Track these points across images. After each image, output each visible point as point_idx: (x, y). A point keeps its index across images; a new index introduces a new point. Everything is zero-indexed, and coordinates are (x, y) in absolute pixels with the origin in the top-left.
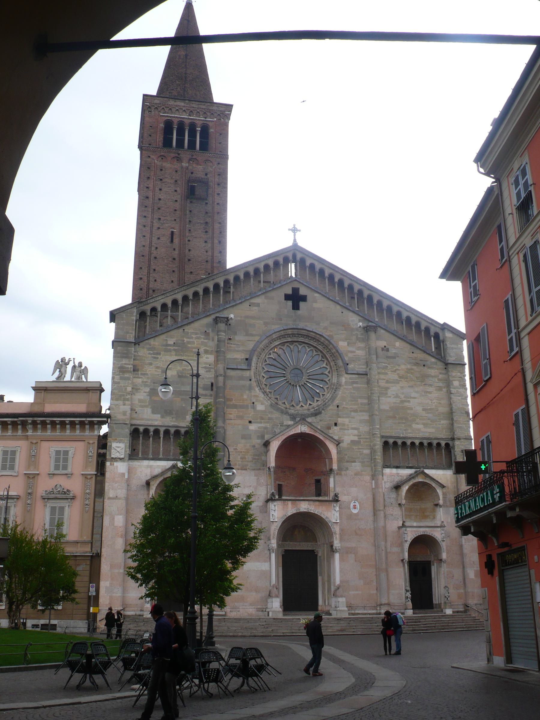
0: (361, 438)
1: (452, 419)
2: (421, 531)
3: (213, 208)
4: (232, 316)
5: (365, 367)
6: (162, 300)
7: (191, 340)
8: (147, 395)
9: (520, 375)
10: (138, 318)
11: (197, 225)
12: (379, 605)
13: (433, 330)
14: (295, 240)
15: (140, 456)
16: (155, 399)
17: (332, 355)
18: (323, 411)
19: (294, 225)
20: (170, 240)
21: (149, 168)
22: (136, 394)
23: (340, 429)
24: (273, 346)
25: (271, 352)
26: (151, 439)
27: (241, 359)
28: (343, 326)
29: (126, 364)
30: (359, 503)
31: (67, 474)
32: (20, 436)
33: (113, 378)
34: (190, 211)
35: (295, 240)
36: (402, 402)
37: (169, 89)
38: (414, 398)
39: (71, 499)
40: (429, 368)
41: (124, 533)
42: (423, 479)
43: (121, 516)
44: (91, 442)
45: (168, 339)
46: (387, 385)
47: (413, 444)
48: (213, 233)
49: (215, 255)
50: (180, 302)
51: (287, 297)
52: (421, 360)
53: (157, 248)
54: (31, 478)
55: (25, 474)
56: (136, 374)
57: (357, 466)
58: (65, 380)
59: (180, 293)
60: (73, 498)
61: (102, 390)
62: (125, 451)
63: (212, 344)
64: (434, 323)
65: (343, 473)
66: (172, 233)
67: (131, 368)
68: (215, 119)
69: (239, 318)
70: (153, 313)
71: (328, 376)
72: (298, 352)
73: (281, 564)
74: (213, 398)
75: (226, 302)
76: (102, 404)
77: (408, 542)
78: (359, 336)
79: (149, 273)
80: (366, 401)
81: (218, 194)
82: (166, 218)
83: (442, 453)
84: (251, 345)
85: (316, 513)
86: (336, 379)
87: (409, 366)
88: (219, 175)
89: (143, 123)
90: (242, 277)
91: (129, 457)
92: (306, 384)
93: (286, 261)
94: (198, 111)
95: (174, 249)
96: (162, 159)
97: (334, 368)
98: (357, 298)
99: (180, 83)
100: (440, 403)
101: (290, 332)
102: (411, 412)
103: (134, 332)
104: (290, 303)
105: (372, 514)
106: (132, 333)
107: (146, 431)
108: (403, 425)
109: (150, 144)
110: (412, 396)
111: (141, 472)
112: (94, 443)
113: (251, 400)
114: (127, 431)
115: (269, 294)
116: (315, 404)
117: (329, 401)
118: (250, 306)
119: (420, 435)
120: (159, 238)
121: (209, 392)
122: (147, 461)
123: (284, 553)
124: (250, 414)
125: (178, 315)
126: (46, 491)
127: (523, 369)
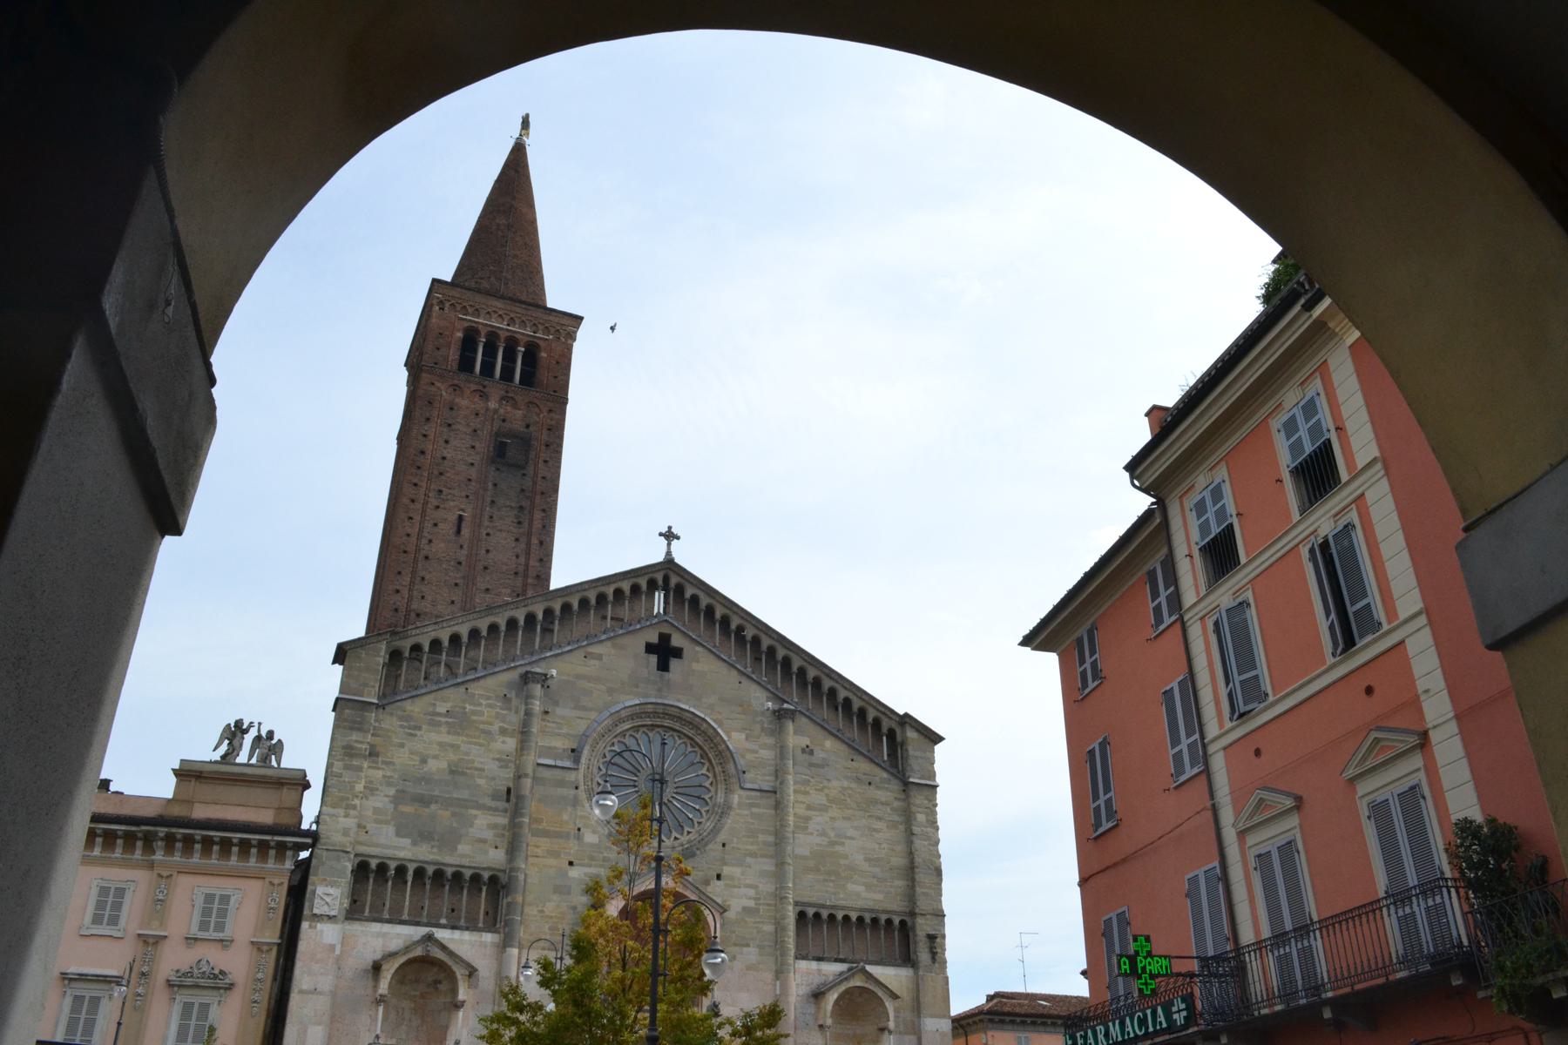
0: (760, 904)
1: (913, 880)
3: (535, 483)
4: (554, 672)
5: (772, 778)
6: (433, 633)
7: (479, 709)
9: (1209, 814)
10: (387, 661)
11: (504, 509)
13: (886, 725)
14: (669, 553)
15: (366, 914)
16: (403, 810)
17: (720, 754)
18: (698, 852)
19: (670, 528)
20: (455, 529)
21: (430, 403)
22: (370, 798)
23: (726, 885)
24: (618, 732)
25: (615, 740)
26: (390, 883)
27: (564, 750)
29: (356, 741)
31: (222, 941)
32: (137, 860)
34: (495, 485)
35: (669, 553)
36: (832, 844)
37: (476, 276)
38: (852, 838)
39: (226, 989)
40: (878, 788)
42: (862, 981)
43: (320, 1028)
44: (276, 881)
45: (438, 703)
46: (809, 813)
47: (846, 918)
49: (532, 563)
50: (465, 639)
51: (650, 648)
52: (865, 774)
53: (430, 541)
54: (151, 942)
55: (139, 935)
56: (373, 762)
57: (751, 954)
58: (238, 760)
59: (467, 624)
60: (230, 987)
61: (307, 786)
62: (341, 904)
63: (514, 720)
64: (888, 713)
66: (460, 518)
67: (366, 749)
68: (551, 337)
70: (414, 655)
71: (709, 791)
74: (508, 814)
75: (543, 649)
76: (304, 810)
80: (771, 839)
81: (546, 462)
82: (450, 491)
83: (894, 938)
84: (582, 726)
86: (723, 795)
87: (846, 784)
88: (549, 429)
89: (425, 327)
90: (576, 605)
91: (346, 914)
93: (653, 585)
94: (524, 319)
95: (461, 547)
96: (455, 390)
97: (720, 778)
99: (495, 269)
100: (893, 850)
101: (650, 708)
102: (846, 862)
103: (377, 685)
104: (654, 659)
106: (374, 687)
107: (382, 868)
108: (831, 884)
109: (436, 364)
110: (848, 834)
111: (365, 944)
112: (282, 883)
115: (619, 641)
116: (684, 839)
117: (709, 834)
118: (585, 657)
119: (860, 904)
120: (436, 525)
121: (502, 804)
124: (573, 847)
125: (458, 663)
126: (178, 971)
127: (1214, 805)
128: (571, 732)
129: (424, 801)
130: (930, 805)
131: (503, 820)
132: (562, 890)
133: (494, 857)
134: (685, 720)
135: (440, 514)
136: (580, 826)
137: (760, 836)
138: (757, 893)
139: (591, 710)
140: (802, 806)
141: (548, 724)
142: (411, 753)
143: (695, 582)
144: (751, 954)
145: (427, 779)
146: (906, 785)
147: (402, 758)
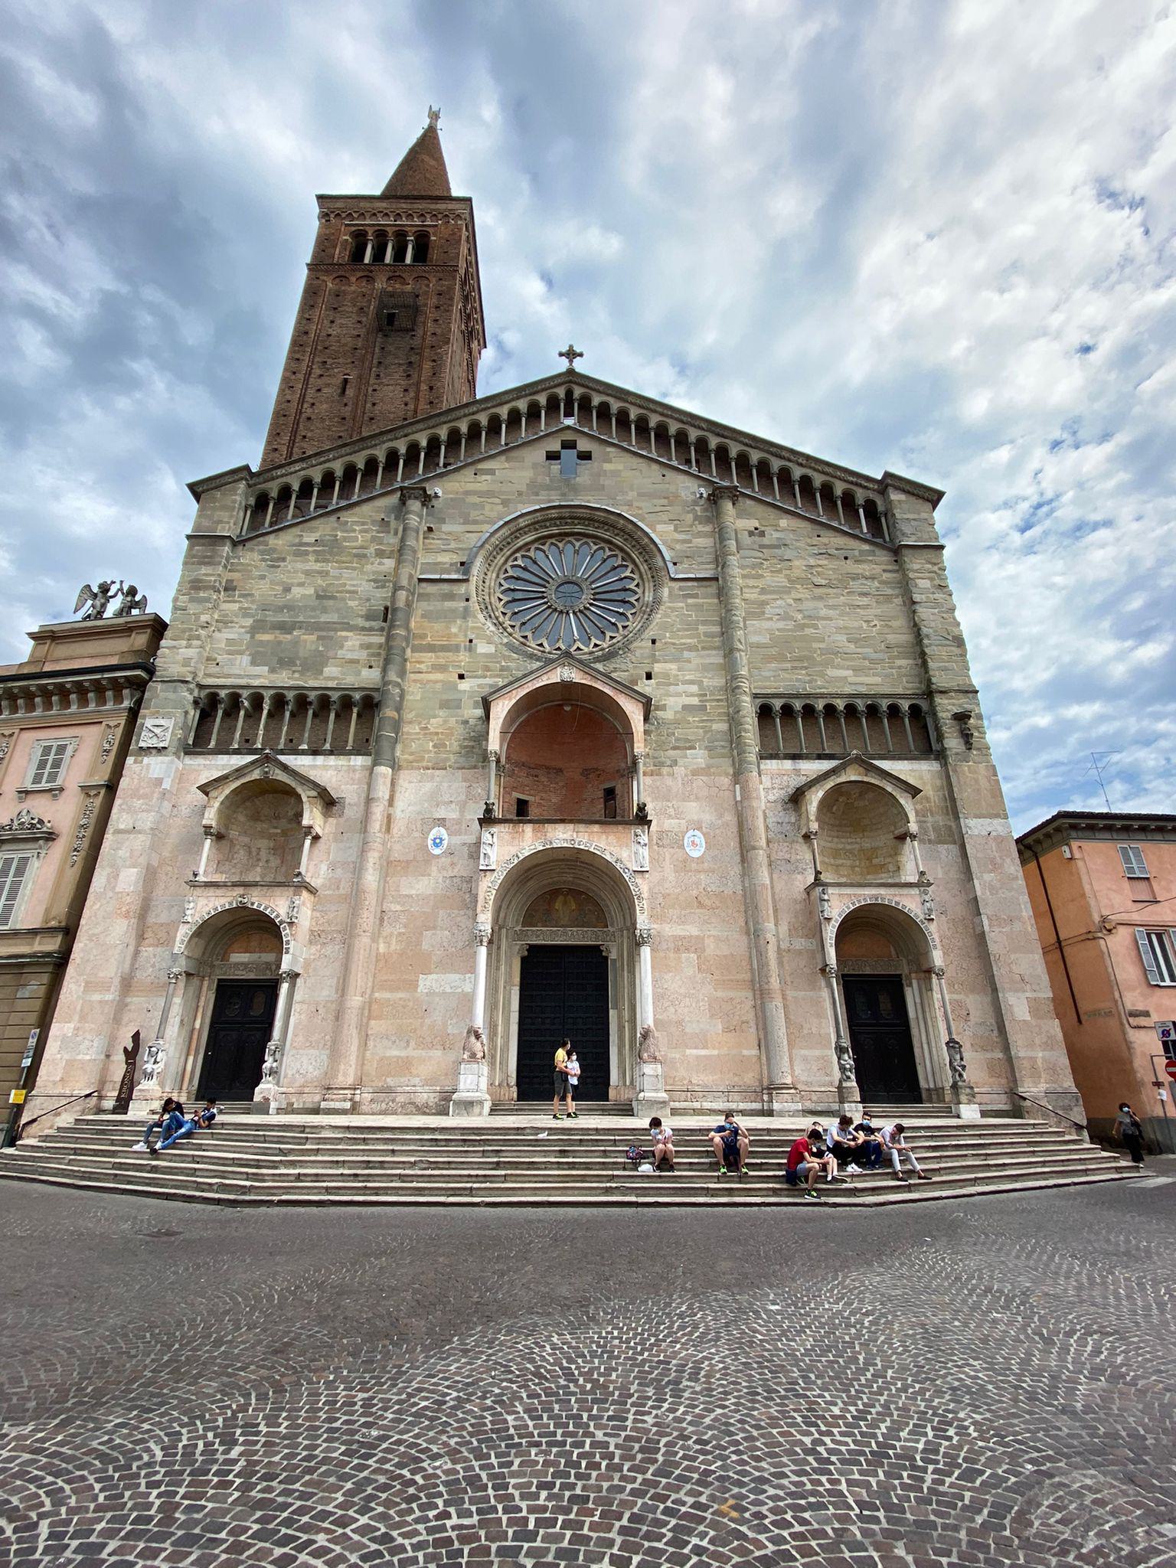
0: (707, 701)
1: (923, 654)
2: (866, 895)
3: (424, 339)
5: (712, 566)
8: (247, 632)
12: (769, 1089)
13: (861, 496)
20: (339, 391)
24: (521, 543)
25: (518, 555)
27: (451, 564)
30: (704, 835)
33: (175, 600)
36: (803, 627)
40: (857, 561)
41: (135, 907)
44: (112, 724)
46: (763, 597)
48: (420, 376)
49: (420, 407)
52: (837, 549)
53: (313, 404)
65: (665, 770)
66: (346, 381)
71: (636, 593)
72: (577, 552)
73: (517, 980)
77: (833, 922)
79: (292, 442)
80: (716, 629)
84: (473, 540)
85: (592, 850)
87: (812, 562)
98: (697, 461)
101: (554, 513)
102: (822, 645)
105: (738, 858)
112: (117, 726)
113: (466, 636)
114: (187, 696)
119: (848, 690)
122: (226, 757)
123: (526, 953)
129: (285, 628)
130: (936, 568)
131: (382, 640)
132: (451, 704)
133: (369, 677)
134: (598, 521)
135: (325, 380)
138: (700, 689)
140: (754, 590)
142: (272, 582)
143: (601, 389)
144: (698, 757)
145: (290, 607)
146: (897, 552)
147: (263, 589)
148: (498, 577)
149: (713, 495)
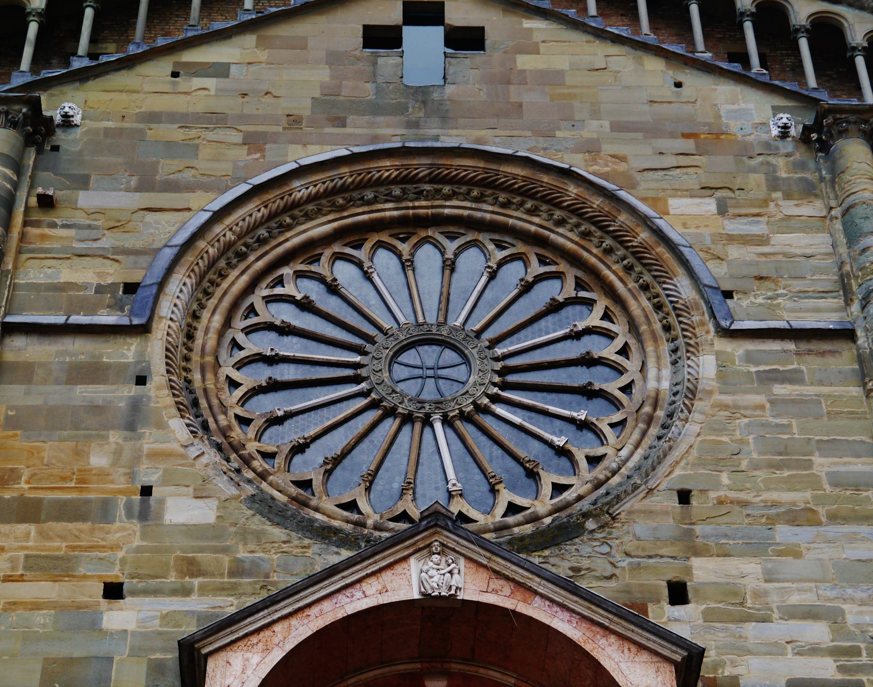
23: (709, 616)
25: (287, 271)
28: (686, 136)
69: (110, 124)
71: (620, 371)
78: (784, 175)
86: (667, 372)
92: (486, 411)
101: (387, 168)
113: (132, 476)
118: (175, 75)
128: (129, 241)
134: (509, 189)
136: (146, 480)
137: (817, 459)
139: (190, 188)
141: (47, 231)
148: (227, 323)
149: (817, 126)
